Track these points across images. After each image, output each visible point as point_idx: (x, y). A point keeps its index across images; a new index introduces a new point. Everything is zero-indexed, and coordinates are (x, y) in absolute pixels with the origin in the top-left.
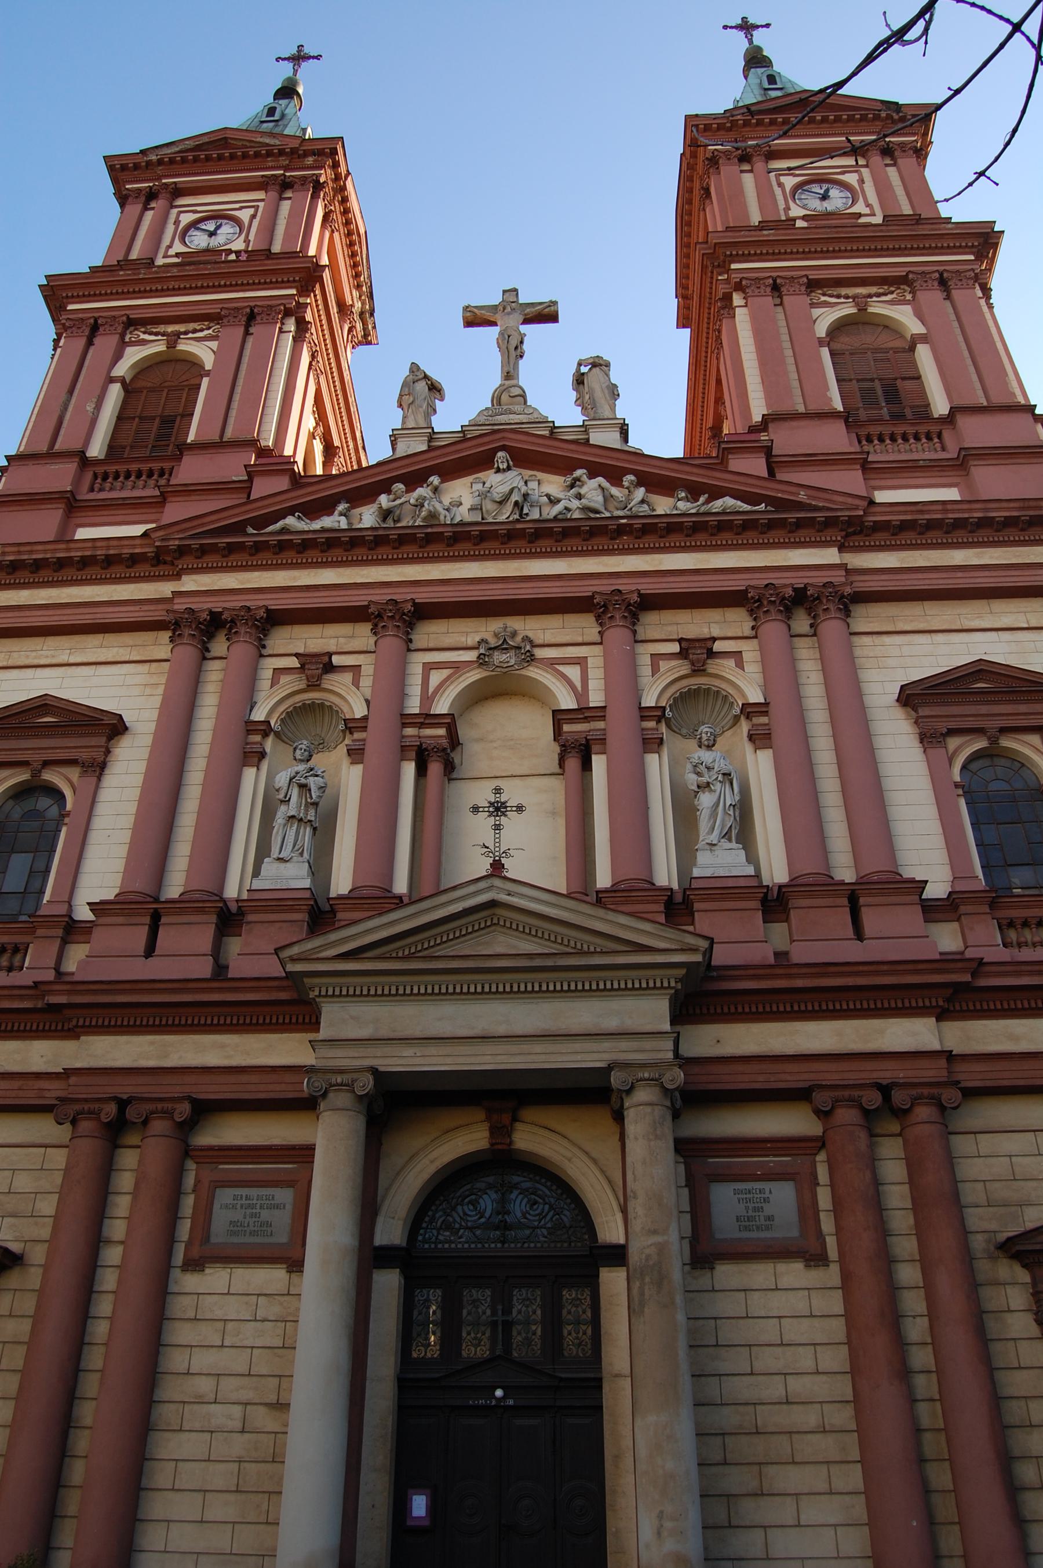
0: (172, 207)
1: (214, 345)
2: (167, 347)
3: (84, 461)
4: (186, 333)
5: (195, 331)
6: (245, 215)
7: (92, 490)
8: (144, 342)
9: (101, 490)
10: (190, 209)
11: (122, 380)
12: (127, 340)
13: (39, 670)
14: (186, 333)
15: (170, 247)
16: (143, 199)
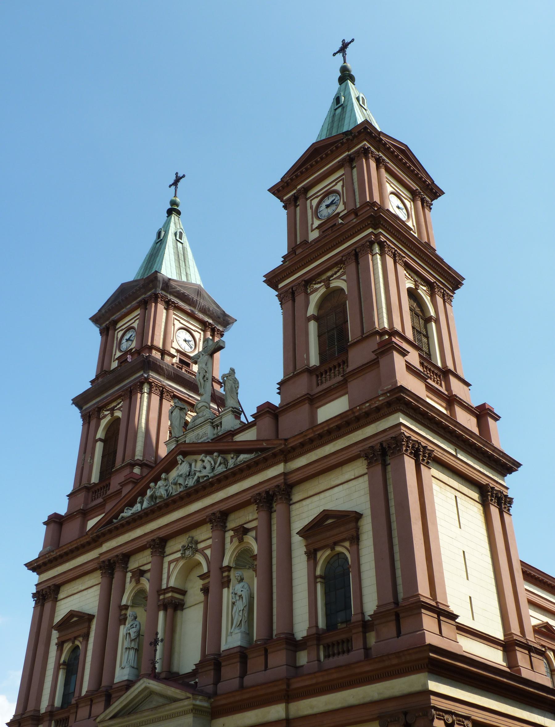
0: (307, 199)
1: (344, 277)
2: (326, 288)
3: (310, 371)
4: (332, 276)
5: (336, 273)
6: (339, 187)
7: (318, 385)
8: (317, 290)
9: (322, 383)
10: (315, 196)
11: (314, 318)
12: (309, 292)
13: (322, 495)
14: (332, 276)
15: (312, 224)
16: (293, 203)
